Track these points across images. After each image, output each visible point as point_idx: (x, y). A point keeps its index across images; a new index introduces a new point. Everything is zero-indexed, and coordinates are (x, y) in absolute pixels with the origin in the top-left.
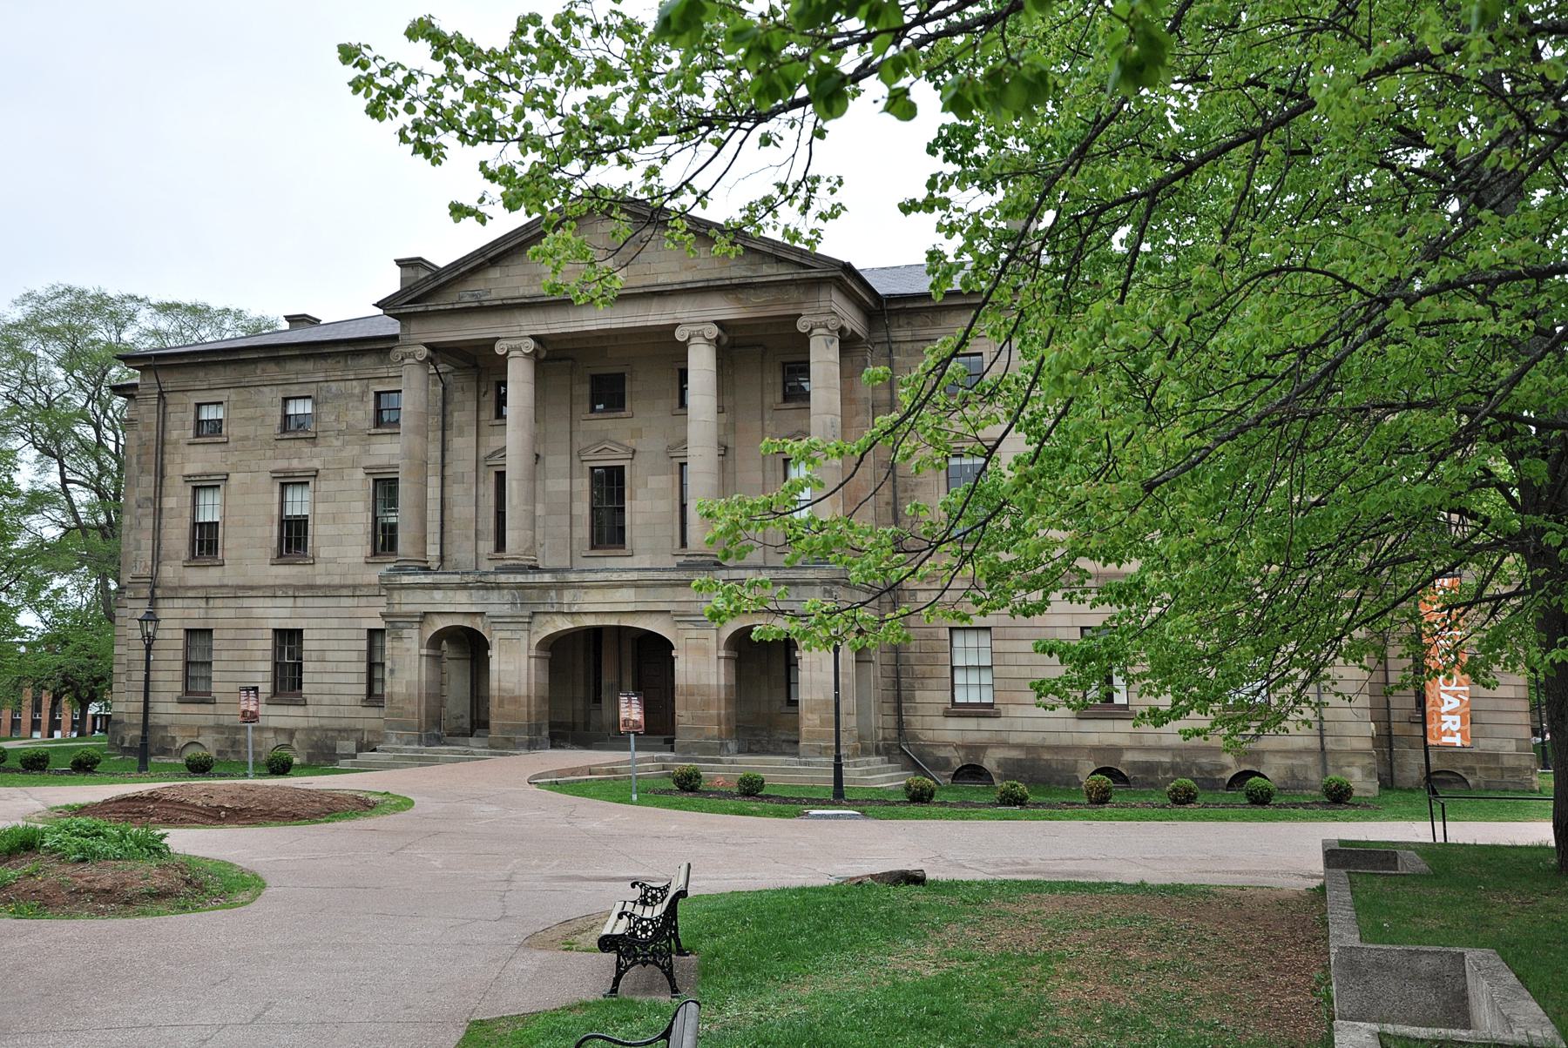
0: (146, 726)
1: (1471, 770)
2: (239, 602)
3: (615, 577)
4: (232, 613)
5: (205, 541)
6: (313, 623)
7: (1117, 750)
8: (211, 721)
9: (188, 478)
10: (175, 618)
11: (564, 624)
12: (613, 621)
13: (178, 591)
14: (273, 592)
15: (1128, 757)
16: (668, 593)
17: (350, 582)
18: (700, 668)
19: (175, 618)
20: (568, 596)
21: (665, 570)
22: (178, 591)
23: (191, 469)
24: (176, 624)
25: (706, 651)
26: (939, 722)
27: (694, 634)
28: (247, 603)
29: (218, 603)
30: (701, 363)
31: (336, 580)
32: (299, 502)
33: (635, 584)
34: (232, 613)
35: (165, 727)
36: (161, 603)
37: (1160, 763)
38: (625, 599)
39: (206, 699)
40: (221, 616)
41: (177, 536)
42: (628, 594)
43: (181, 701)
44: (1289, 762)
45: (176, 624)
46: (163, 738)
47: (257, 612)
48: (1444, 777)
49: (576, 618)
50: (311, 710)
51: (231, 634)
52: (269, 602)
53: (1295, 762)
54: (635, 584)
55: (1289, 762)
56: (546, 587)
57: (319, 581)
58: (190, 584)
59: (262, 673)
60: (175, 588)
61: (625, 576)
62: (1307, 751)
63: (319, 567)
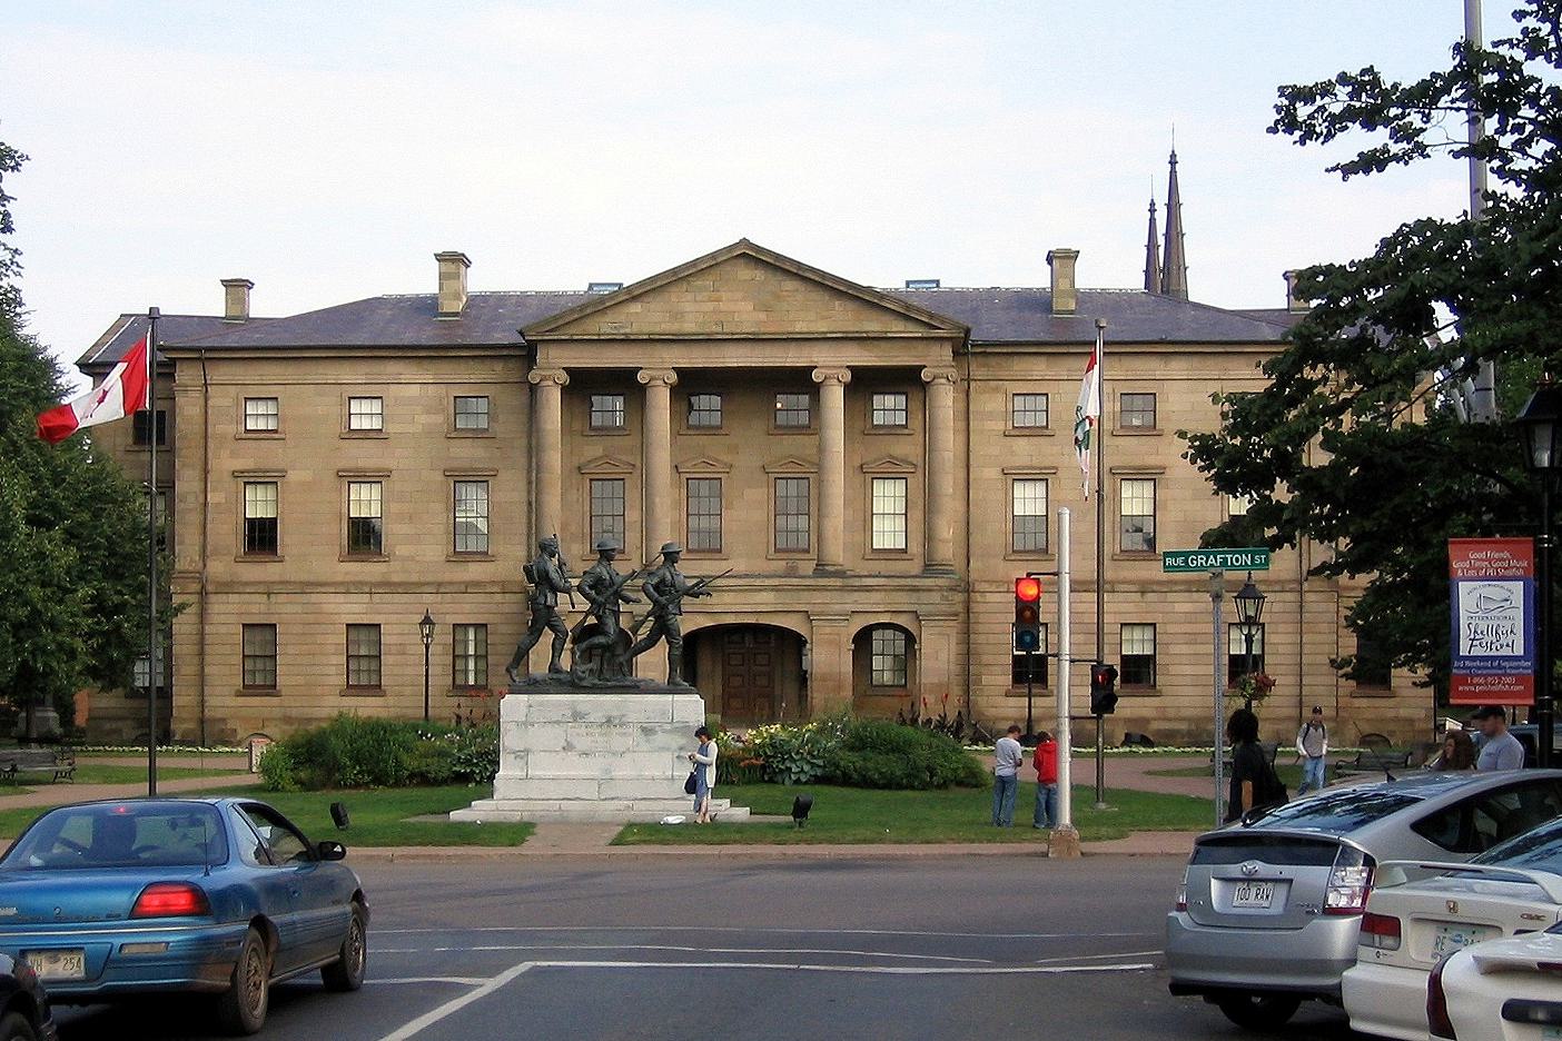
0: (202, 721)
1: (1392, 733)
2: (305, 598)
3: (758, 582)
4: (298, 608)
5: (262, 537)
6: (394, 618)
7: (1146, 721)
8: (277, 713)
9: (235, 475)
10: (227, 616)
11: (708, 622)
12: (751, 620)
13: (228, 587)
14: (348, 588)
15: (1155, 726)
17: (430, 578)
19: (227, 616)
22: (228, 587)
23: (239, 464)
24: (233, 619)
25: (839, 645)
26: (1002, 701)
28: (314, 598)
29: (282, 598)
31: (414, 578)
32: (365, 501)
33: (775, 589)
34: (298, 608)
35: (223, 720)
36: (213, 598)
37: (1178, 731)
38: (765, 600)
39: (270, 689)
40: (285, 611)
41: (228, 535)
43: (239, 694)
44: (1276, 727)
45: (233, 619)
46: (223, 730)
47: (326, 608)
48: (1374, 738)
49: (717, 617)
50: (391, 700)
51: (297, 629)
52: (341, 598)
53: (1280, 727)
55: (1276, 727)
57: (395, 578)
58: (244, 579)
59: (333, 669)
60: (226, 584)
61: (768, 582)
62: (1289, 718)
63: (395, 565)
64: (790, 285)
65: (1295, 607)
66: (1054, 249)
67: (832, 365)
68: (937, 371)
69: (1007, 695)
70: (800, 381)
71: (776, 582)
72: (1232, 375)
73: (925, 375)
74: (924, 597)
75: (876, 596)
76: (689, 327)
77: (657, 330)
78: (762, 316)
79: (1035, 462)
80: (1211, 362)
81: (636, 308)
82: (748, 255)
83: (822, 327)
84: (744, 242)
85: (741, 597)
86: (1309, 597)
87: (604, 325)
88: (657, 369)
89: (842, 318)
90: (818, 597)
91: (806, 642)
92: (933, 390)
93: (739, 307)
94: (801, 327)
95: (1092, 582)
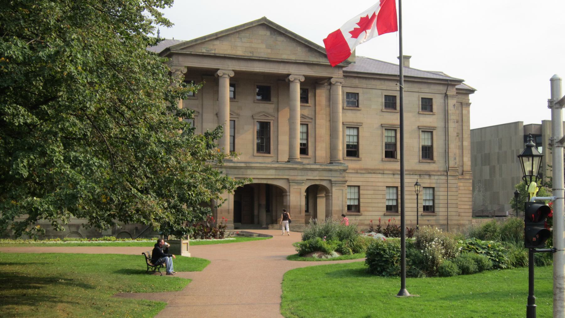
3: (269, 165)
16: (287, 172)
18: (296, 198)
20: (249, 172)
21: (257, 163)
27: (296, 187)
30: (297, 90)
38: (271, 174)
42: (272, 172)
54: (276, 169)
56: (240, 168)
64: (280, 39)
65: (445, 181)
66: (326, 37)
67: (298, 74)
68: (337, 80)
69: (384, 215)
70: (283, 81)
71: (323, 167)
72: (423, 90)
73: (332, 80)
74: (334, 174)
75: (316, 173)
76: (239, 52)
77: (226, 53)
78: (269, 51)
79: (355, 121)
80: (416, 85)
81: (217, 43)
82: (265, 25)
83: (293, 58)
84: (264, 19)
85: (261, 172)
86: (449, 178)
87: (203, 50)
88: (226, 70)
89: (301, 54)
90: (292, 172)
91: (286, 192)
92: (333, 88)
93: (261, 46)
94: (285, 57)
95: (398, 170)
